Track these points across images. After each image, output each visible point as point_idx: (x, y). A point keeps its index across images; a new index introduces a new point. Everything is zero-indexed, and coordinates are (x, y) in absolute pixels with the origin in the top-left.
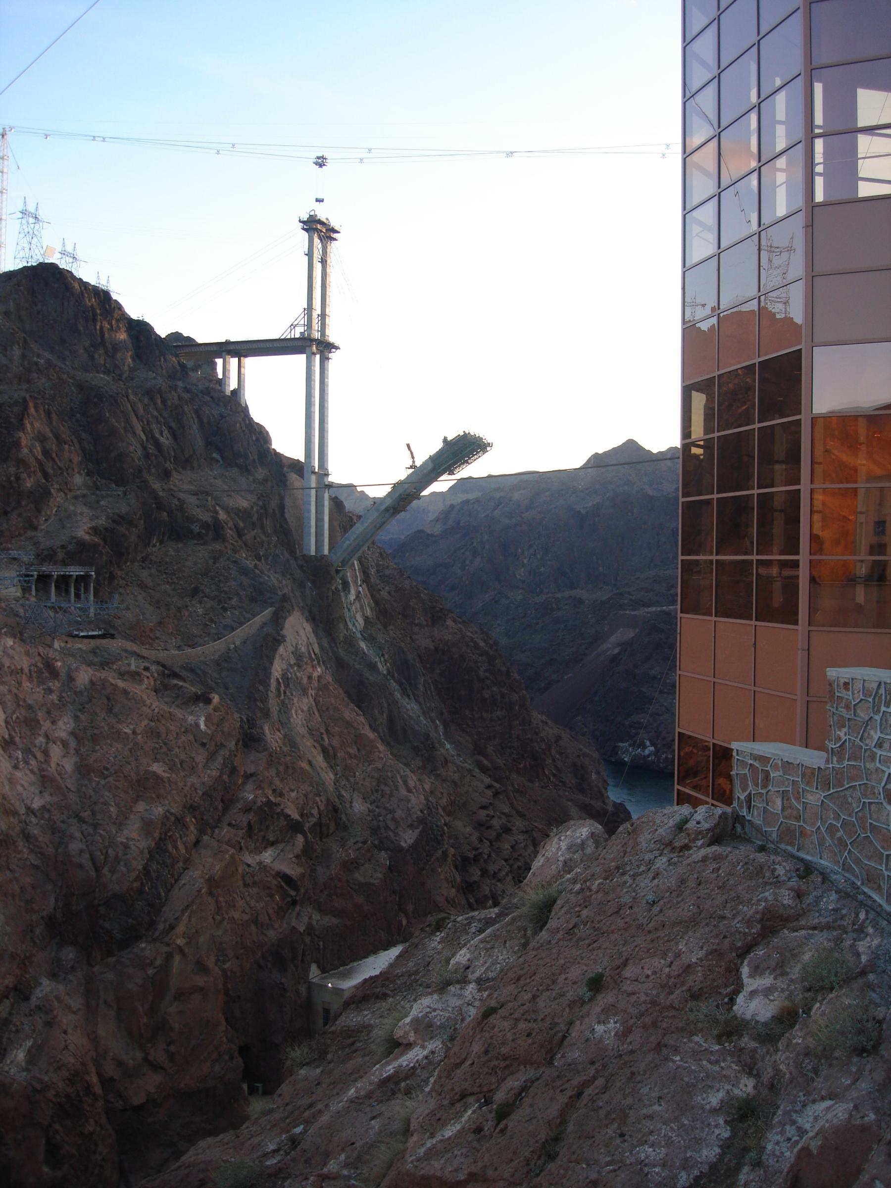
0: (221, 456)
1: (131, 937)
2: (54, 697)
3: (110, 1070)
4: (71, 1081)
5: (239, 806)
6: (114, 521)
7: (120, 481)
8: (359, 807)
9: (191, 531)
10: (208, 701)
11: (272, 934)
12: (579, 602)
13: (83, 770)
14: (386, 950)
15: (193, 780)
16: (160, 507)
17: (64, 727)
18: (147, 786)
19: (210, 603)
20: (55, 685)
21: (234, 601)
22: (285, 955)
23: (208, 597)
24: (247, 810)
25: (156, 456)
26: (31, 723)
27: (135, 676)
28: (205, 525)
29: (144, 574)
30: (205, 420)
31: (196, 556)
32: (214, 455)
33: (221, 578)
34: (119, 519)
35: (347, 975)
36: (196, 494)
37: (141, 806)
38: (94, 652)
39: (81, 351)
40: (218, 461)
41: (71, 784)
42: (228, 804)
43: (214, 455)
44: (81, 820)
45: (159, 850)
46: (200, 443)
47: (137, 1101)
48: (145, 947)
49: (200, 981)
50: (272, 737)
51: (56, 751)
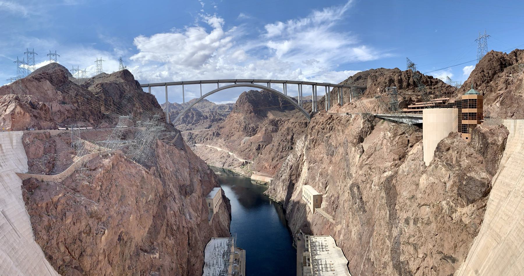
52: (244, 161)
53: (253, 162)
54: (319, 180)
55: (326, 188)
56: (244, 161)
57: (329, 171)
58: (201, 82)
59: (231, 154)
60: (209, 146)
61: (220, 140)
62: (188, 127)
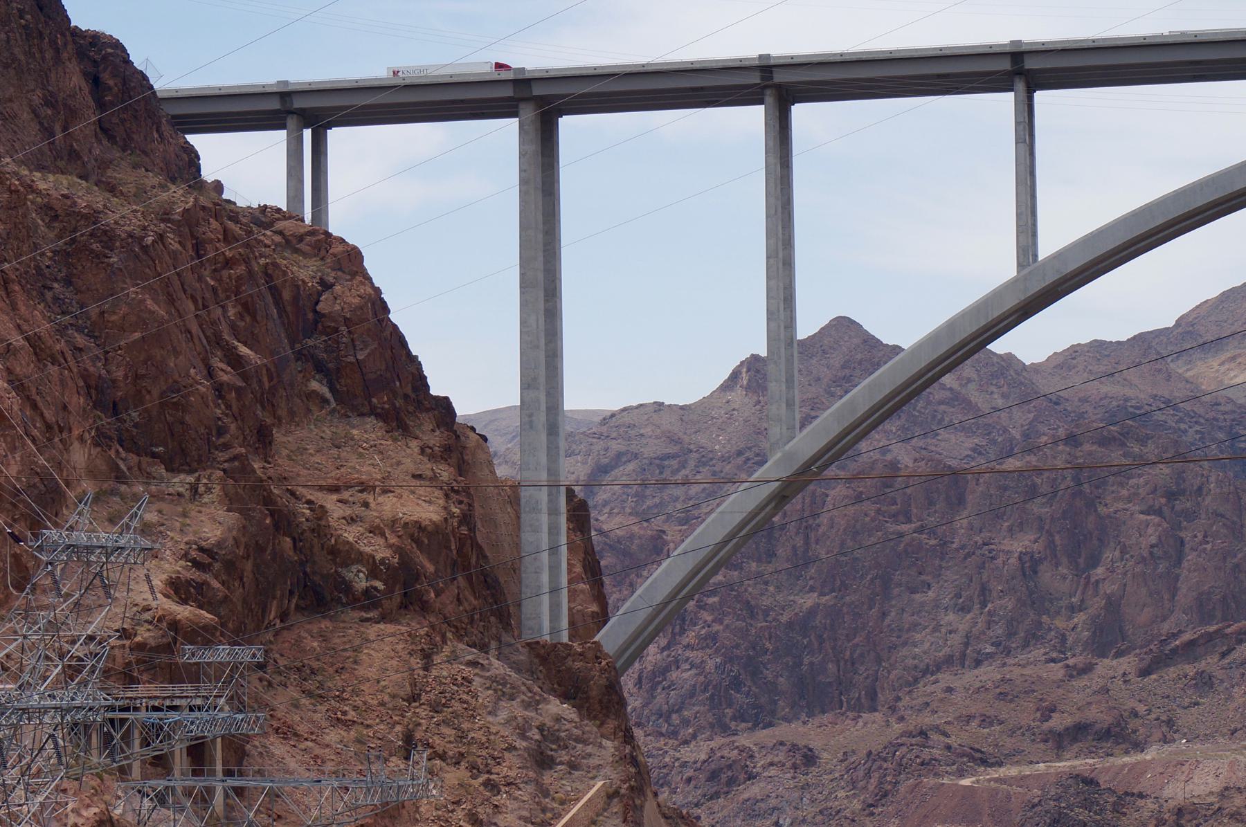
0: (332, 389)
6: (196, 564)
9: (347, 587)
12: (810, 758)
16: (282, 521)
19: (454, 776)
21: (510, 767)
23: (443, 757)
25: (239, 391)
29: (281, 700)
30: (287, 295)
32: (314, 385)
33: (457, 706)
34: (203, 558)
36: (335, 489)
39: (26, 116)
40: (325, 401)
43: (314, 385)
58: (1023, 71)
62: (1080, 702)
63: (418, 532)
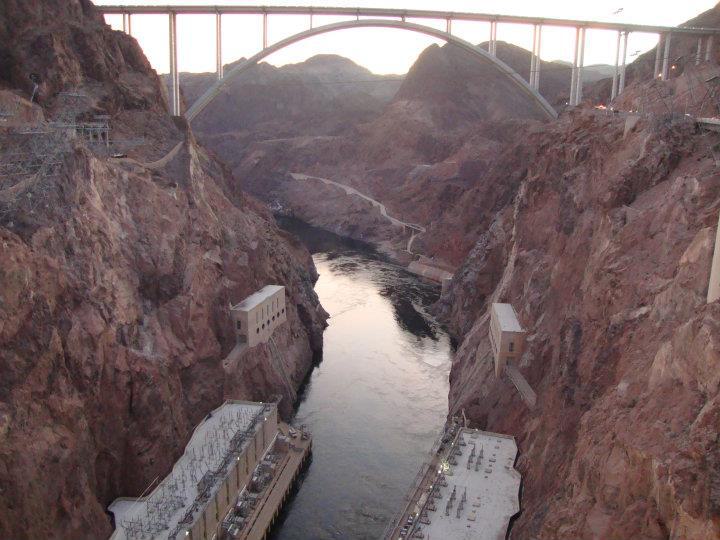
1: (175, 292)
2: (115, 186)
3: (176, 353)
4: (169, 357)
5: (194, 234)
7: (100, 79)
8: (231, 233)
9: (133, 104)
10: (175, 186)
11: (217, 290)
12: (233, 138)
13: (137, 220)
14: (252, 294)
15: (178, 222)
17: (123, 200)
18: (164, 226)
20: (115, 180)
22: (223, 299)
24: (198, 235)
26: (111, 199)
27: (144, 175)
28: (140, 101)
31: (140, 117)
34: (105, 99)
35: (243, 306)
37: (165, 235)
38: (121, 164)
41: (133, 226)
42: (190, 234)
44: (143, 243)
45: (177, 253)
46: (122, 60)
47: (187, 364)
48: (181, 298)
49: (200, 311)
50: (198, 202)
51: (123, 211)
52: (403, 224)
53: (424, 230)
54: (528, 295)
55: (537, 317)
56: (403, 224)
57: (552, 277)
58: (265, 11)
59: (375, 203)
60: (327, 182)
61: (354, 167)
63: (149, 95)
